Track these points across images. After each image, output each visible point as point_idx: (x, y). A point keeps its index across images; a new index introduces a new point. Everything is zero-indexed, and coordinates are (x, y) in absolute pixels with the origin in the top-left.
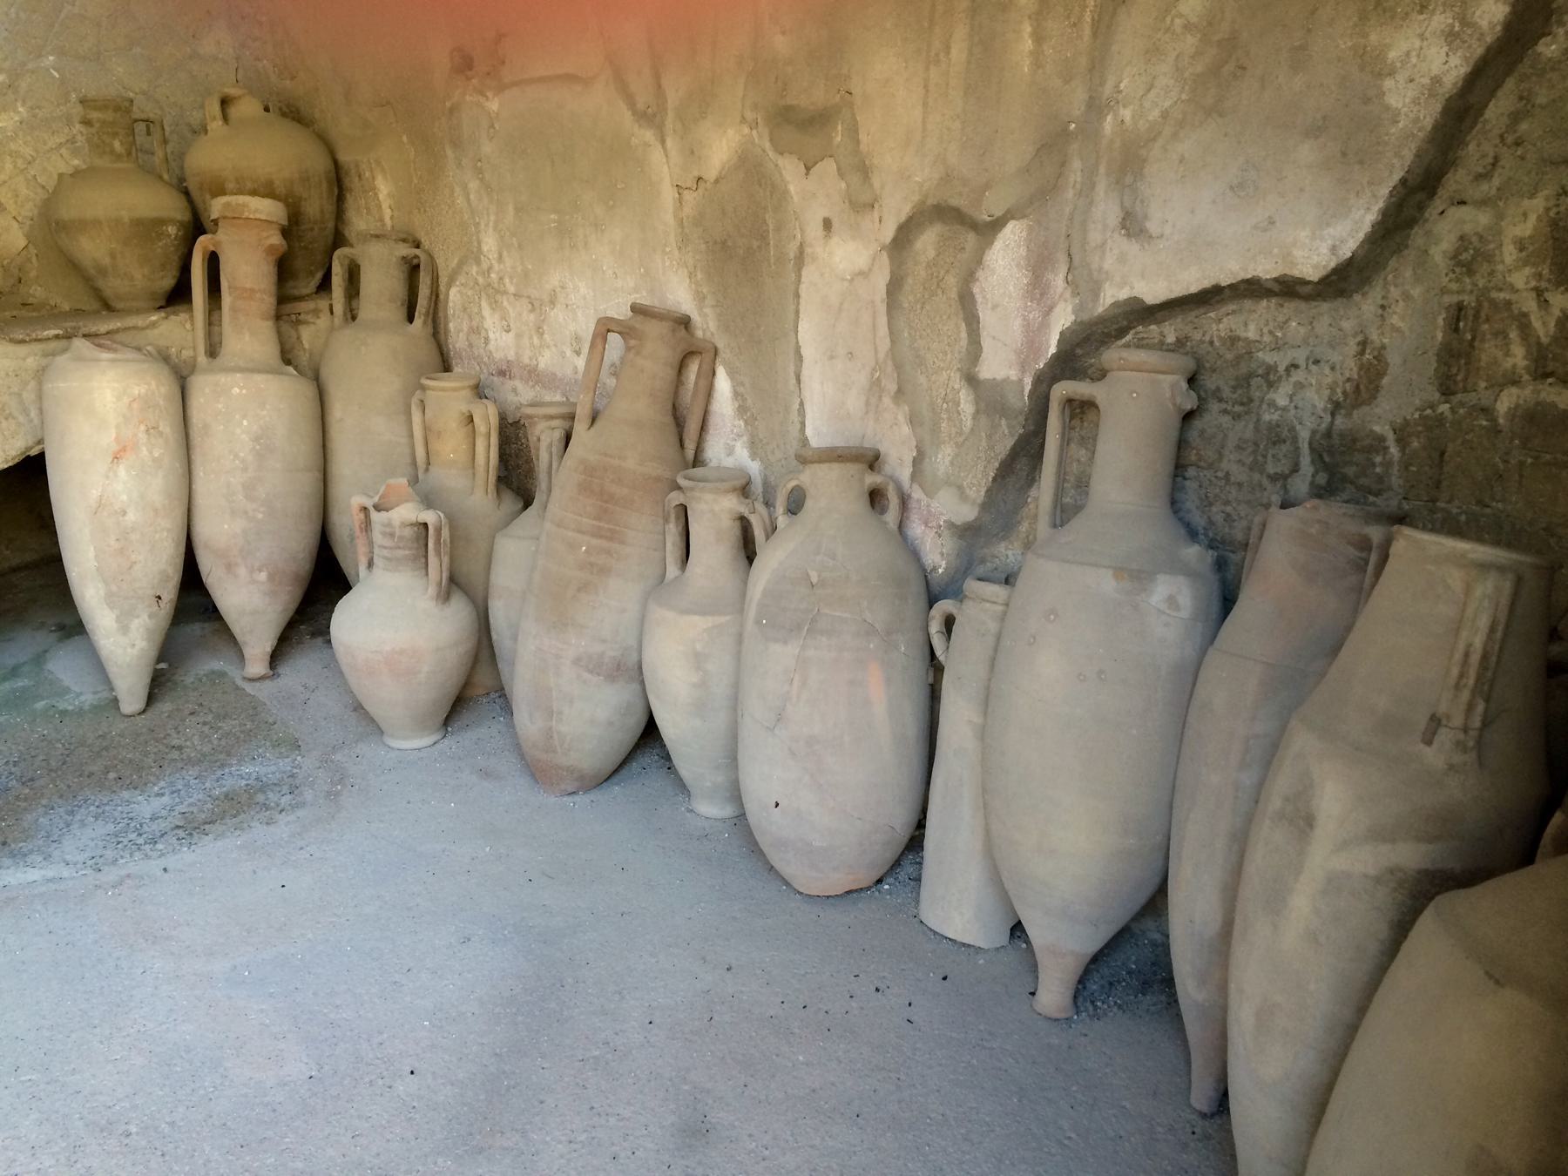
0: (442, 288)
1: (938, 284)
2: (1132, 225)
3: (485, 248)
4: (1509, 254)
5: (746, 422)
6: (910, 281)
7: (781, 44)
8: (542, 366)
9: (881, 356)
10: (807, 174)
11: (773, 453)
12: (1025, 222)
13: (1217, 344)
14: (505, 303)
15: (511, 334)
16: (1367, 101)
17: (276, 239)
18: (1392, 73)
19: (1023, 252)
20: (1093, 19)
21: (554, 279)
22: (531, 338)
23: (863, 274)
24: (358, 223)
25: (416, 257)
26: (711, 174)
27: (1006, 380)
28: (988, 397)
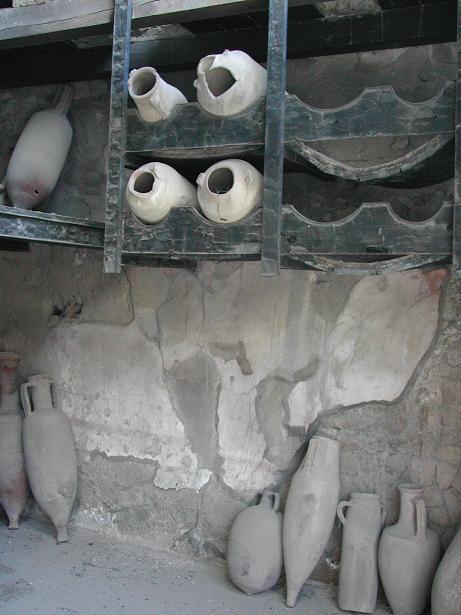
2: (339, 385)
8: (87, 419)
21: (99, 390)
28: (293, 431)
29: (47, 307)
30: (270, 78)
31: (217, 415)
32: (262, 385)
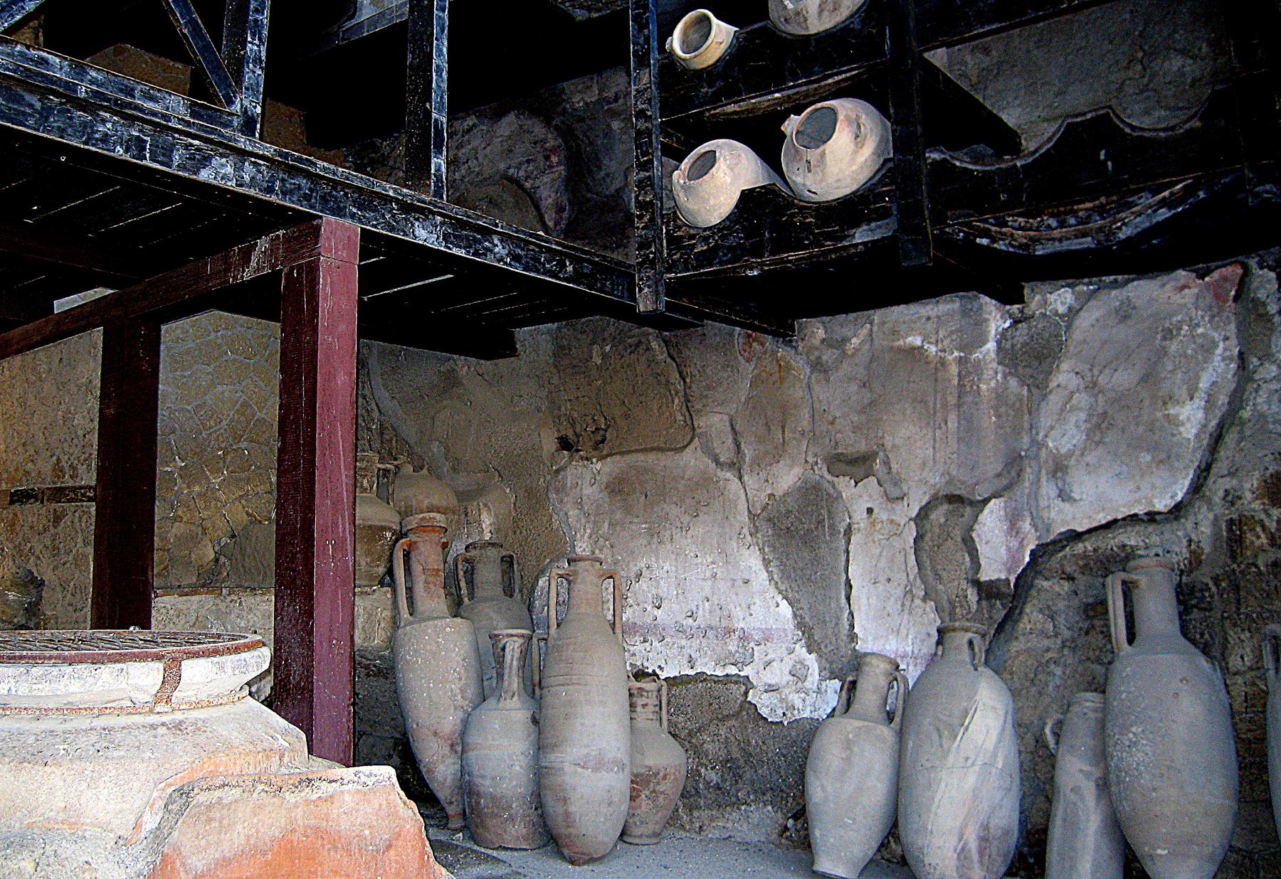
2: (1064, 496)
4: (1248, 495)
9: (911, 577)
11: (826, 646)
12: (1002, 499)
13: (1115, 549)
16: (1173, 435)
18: (1183, 424)
19: (1002, 513)
21: (642, 564)
26: (779, 492)
27: (999, 580)
31: (848, 582)
32: (923, 515)
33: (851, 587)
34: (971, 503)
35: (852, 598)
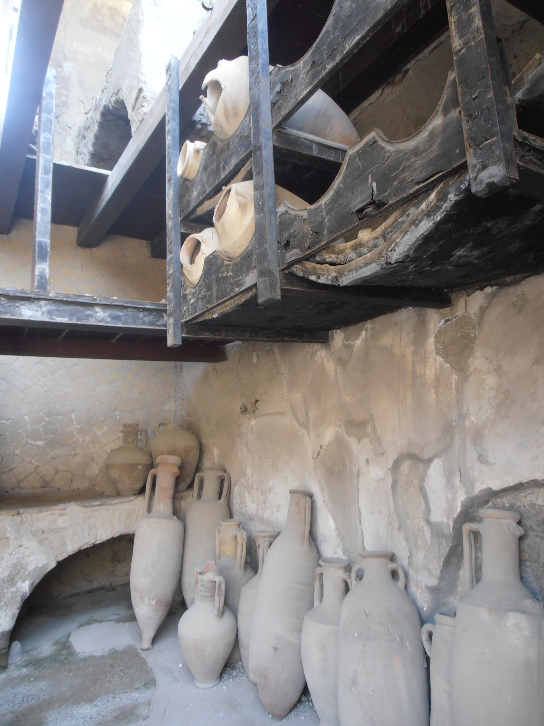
0: (232, 487)
1: (411, 484)
3: (247, 472)
5: (341, 540)
6: (400, 482)
7: (347, 399)
8: (265, 516)
10: (359, 443)
14: (253, 492)
15: (255, 504)
17: (176, 470)
19: (442, 470)
20: (455, 387)
22: (262, 505)
23: (382, 480)
24: (207, 463)
25: (224, 476)
29: (237, 406)
30: (250, 60)
31: (359, 509)
32: (396, 466)
33: (360, 513)
34: (421, 460)
35: (362, 521)
